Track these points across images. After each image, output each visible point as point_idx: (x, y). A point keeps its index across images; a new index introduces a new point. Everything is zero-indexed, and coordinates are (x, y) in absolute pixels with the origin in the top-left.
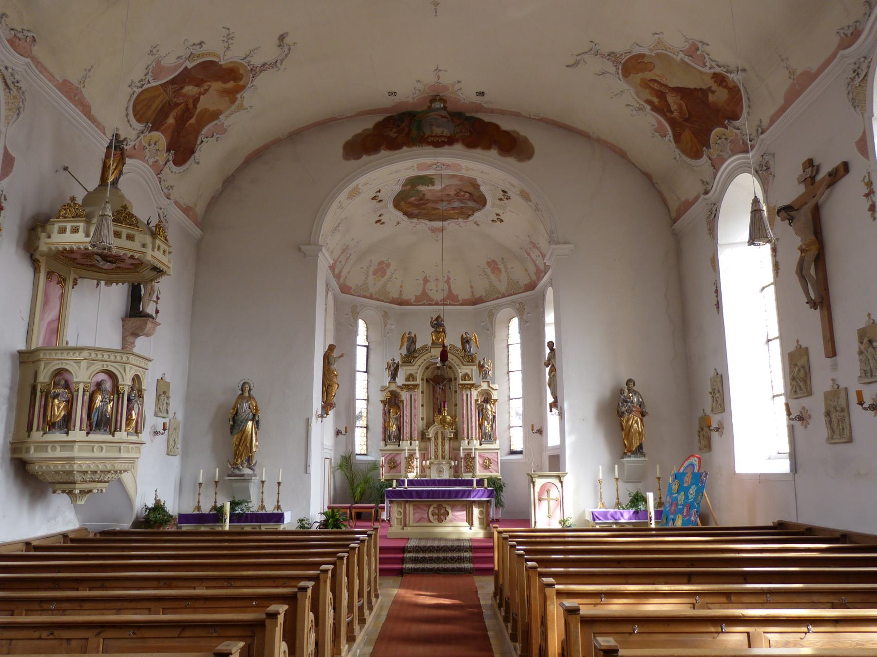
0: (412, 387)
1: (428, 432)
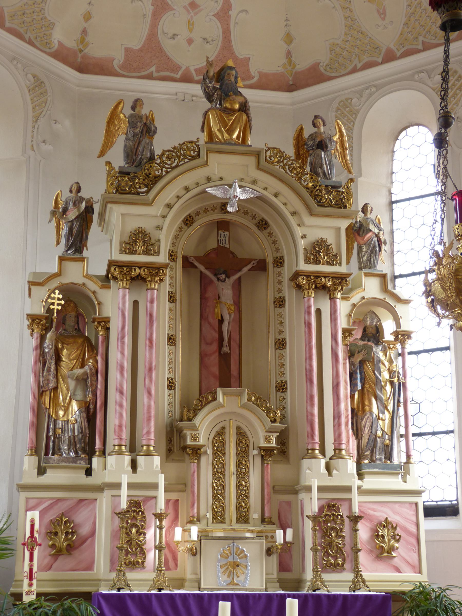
0: (144, 273)
1: (194, 428)
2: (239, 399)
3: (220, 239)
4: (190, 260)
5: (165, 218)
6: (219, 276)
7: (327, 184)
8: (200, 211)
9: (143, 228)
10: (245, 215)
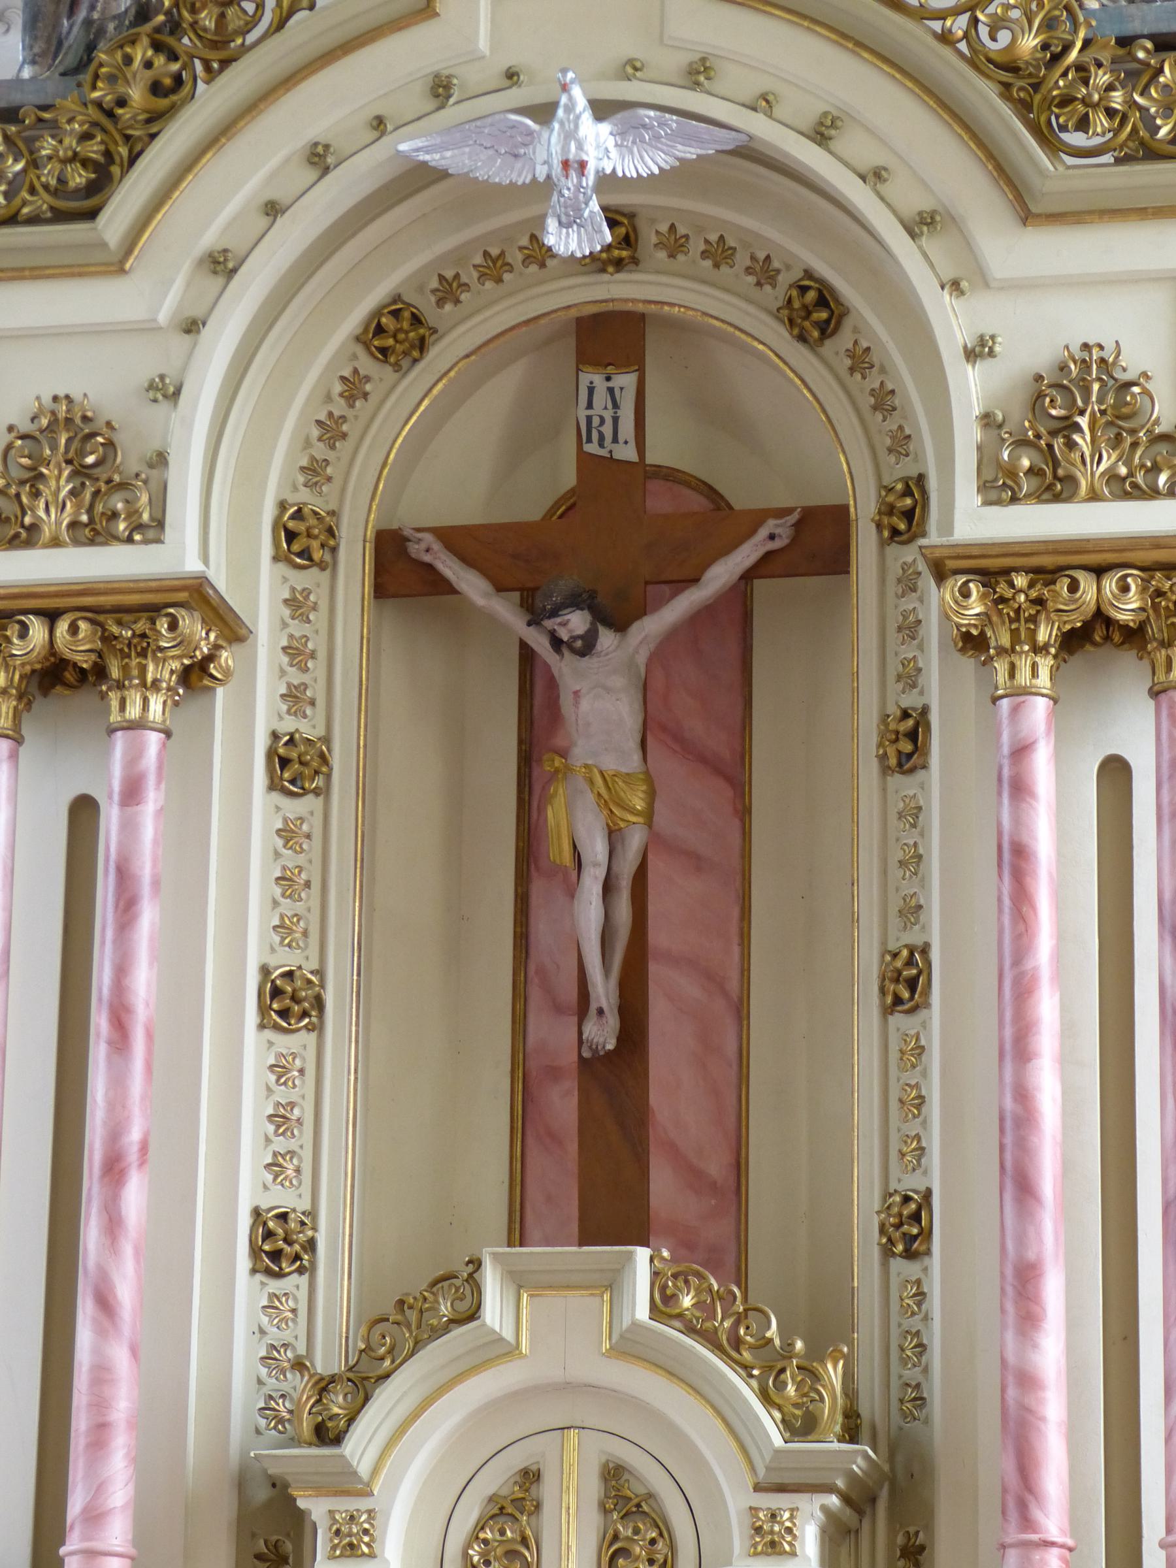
2: (606, 1308)
3: (589, 419)
4: (415, 550)
5: (198, 332)
6: (549, 624)
7: (1134, 27)
8: (457, 276)
9: (77, 395)
10: (717, 266)
